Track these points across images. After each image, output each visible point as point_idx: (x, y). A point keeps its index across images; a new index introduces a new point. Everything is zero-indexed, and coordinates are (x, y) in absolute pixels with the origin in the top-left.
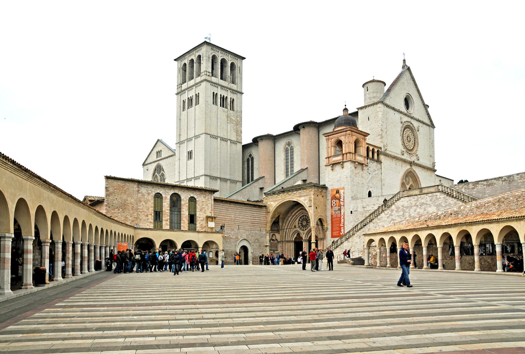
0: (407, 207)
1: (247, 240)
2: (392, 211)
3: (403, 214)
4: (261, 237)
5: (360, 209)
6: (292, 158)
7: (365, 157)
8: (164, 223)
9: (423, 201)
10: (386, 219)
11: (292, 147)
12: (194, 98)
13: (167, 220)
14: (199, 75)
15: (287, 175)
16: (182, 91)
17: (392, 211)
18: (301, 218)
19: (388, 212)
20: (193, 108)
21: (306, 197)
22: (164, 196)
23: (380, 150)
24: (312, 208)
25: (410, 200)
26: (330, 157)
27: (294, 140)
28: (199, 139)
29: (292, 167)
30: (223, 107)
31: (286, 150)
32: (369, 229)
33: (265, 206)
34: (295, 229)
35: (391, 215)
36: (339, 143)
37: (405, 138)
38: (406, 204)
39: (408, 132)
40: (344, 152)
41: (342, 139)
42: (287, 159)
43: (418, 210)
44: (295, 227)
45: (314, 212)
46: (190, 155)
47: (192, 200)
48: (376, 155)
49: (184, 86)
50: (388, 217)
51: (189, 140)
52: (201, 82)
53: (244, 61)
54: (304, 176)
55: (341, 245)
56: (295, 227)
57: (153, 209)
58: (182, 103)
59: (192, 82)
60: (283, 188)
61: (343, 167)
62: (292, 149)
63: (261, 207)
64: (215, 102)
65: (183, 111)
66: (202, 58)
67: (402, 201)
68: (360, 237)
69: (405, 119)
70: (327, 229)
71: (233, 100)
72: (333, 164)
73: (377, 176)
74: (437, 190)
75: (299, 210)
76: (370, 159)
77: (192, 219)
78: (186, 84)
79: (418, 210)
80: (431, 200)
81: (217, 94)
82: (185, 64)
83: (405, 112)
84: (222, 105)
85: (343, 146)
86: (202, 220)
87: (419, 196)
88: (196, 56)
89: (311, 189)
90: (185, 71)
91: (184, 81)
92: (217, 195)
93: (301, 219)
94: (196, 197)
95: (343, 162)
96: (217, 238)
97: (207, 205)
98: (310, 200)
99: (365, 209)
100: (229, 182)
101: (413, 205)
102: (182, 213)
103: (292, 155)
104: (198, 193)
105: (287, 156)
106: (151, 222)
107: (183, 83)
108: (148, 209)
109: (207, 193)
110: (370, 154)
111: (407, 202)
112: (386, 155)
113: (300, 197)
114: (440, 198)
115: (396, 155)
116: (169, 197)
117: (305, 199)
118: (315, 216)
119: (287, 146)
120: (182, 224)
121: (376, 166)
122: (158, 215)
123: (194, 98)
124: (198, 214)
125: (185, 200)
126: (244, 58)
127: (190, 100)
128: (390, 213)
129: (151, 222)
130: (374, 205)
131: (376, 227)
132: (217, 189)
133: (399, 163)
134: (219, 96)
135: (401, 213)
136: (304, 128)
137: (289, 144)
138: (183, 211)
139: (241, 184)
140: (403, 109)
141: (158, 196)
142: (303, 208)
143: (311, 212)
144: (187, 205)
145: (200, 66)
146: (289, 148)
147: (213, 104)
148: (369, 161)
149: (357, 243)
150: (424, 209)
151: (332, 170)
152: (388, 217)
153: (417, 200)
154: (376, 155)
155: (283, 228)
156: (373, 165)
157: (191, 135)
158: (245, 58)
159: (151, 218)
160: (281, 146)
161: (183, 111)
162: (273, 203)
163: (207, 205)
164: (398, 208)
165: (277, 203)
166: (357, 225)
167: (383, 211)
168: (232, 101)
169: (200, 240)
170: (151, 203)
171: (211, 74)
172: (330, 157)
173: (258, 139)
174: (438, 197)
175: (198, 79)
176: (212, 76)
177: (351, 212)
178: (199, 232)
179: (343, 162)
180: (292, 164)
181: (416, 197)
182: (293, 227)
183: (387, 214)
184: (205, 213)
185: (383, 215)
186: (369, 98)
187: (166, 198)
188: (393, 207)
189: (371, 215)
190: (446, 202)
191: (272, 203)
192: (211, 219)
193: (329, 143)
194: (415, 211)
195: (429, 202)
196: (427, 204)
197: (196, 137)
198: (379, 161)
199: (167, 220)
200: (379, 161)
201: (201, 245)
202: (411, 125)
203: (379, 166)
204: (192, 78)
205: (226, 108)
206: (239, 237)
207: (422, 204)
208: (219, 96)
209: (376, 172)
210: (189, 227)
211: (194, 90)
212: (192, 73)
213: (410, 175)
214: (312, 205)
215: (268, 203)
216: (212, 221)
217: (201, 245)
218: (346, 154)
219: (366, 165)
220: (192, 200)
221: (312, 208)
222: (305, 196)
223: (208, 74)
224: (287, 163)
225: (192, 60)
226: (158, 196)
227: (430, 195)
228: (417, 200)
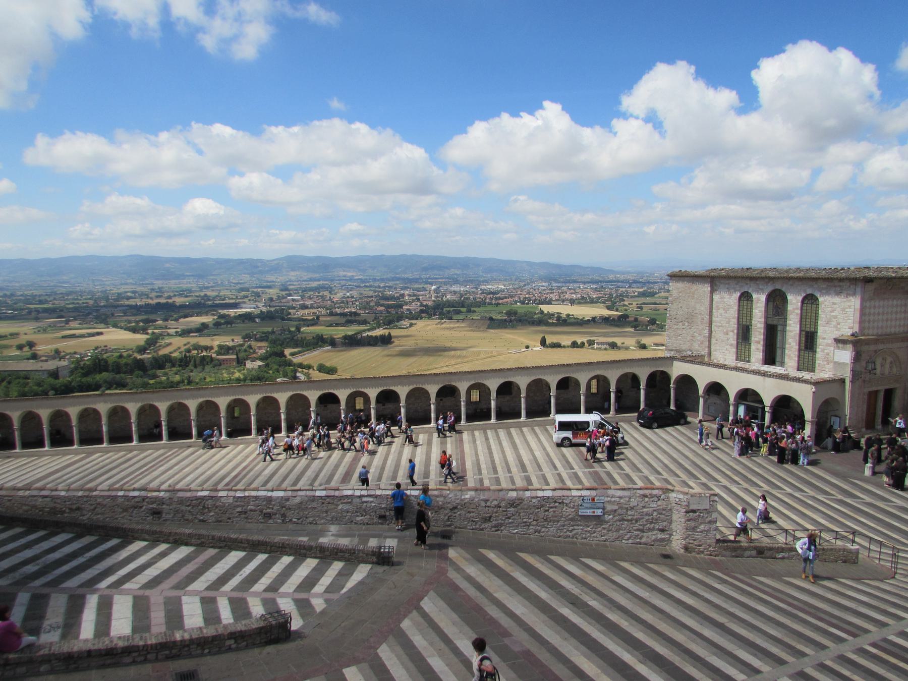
8: (753, 347)
13: (758, 342)
22: (755, 296)
47: (810, 300)
57: (735, 321)
77: (809, 341)
86: (828, 345)
94: (817, 295)
97: (843, 310)
102: (788, 328)
106: (731, 345)
108: (728, 322)
116: (763, 298)
120: (787, 351)
122: (744, 333)
129: (731, 345)
141: (746, 297)
144: (799, 312)
159: (732, 338)
163: (843, 310)
170: (733, 312)
184: (838, 330)
187: (758, 299)
192: (840, 345)
199: (758, 342)
201: (768, 401)
216: (843, 349)
217: (768, 401)
220: (810, 300)
226: (746, 297)
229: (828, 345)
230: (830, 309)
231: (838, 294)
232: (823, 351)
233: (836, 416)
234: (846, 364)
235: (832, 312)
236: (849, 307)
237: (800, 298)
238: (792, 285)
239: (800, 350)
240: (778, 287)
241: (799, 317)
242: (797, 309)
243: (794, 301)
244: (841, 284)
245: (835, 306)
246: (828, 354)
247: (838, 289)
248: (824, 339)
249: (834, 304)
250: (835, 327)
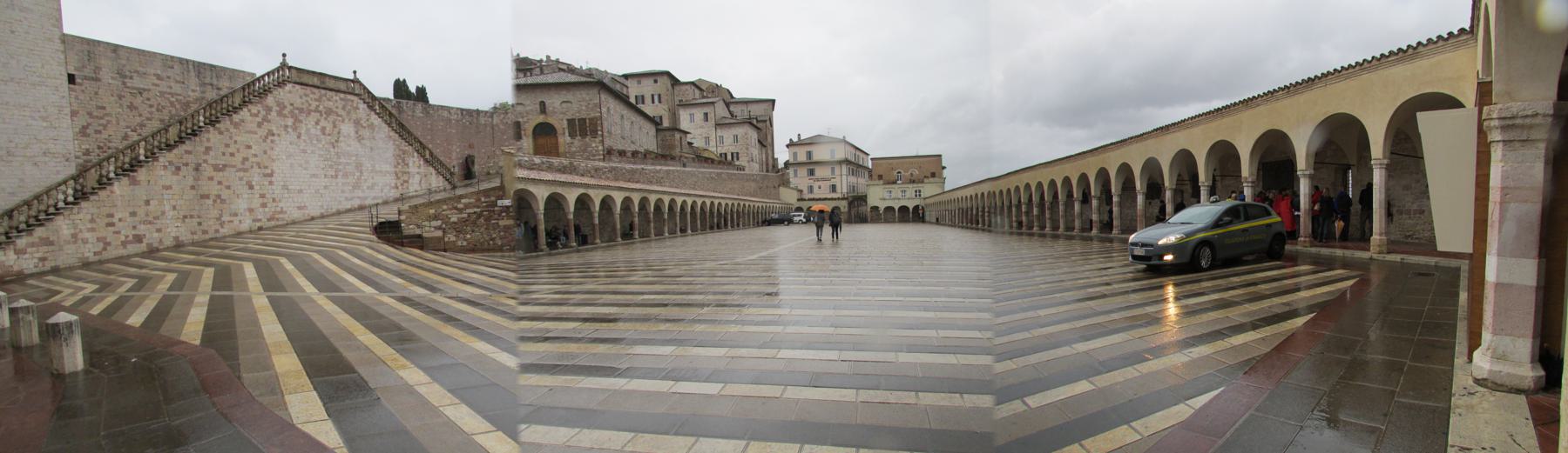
0: (301, 110)
2: (269, 109)
10: (253, 126)
17: (269, 109)
32: (208, 149)
35: (265, 119)
38: (298, 102)
43: (323, 123)
50: (260, 125)
68: (178, 169)
79: (323, 123)
131: (227, 146)
149: (169, 188)
153: (319, 100)
164: (282, 106)
195: (340, 112)
207: (329, 112)
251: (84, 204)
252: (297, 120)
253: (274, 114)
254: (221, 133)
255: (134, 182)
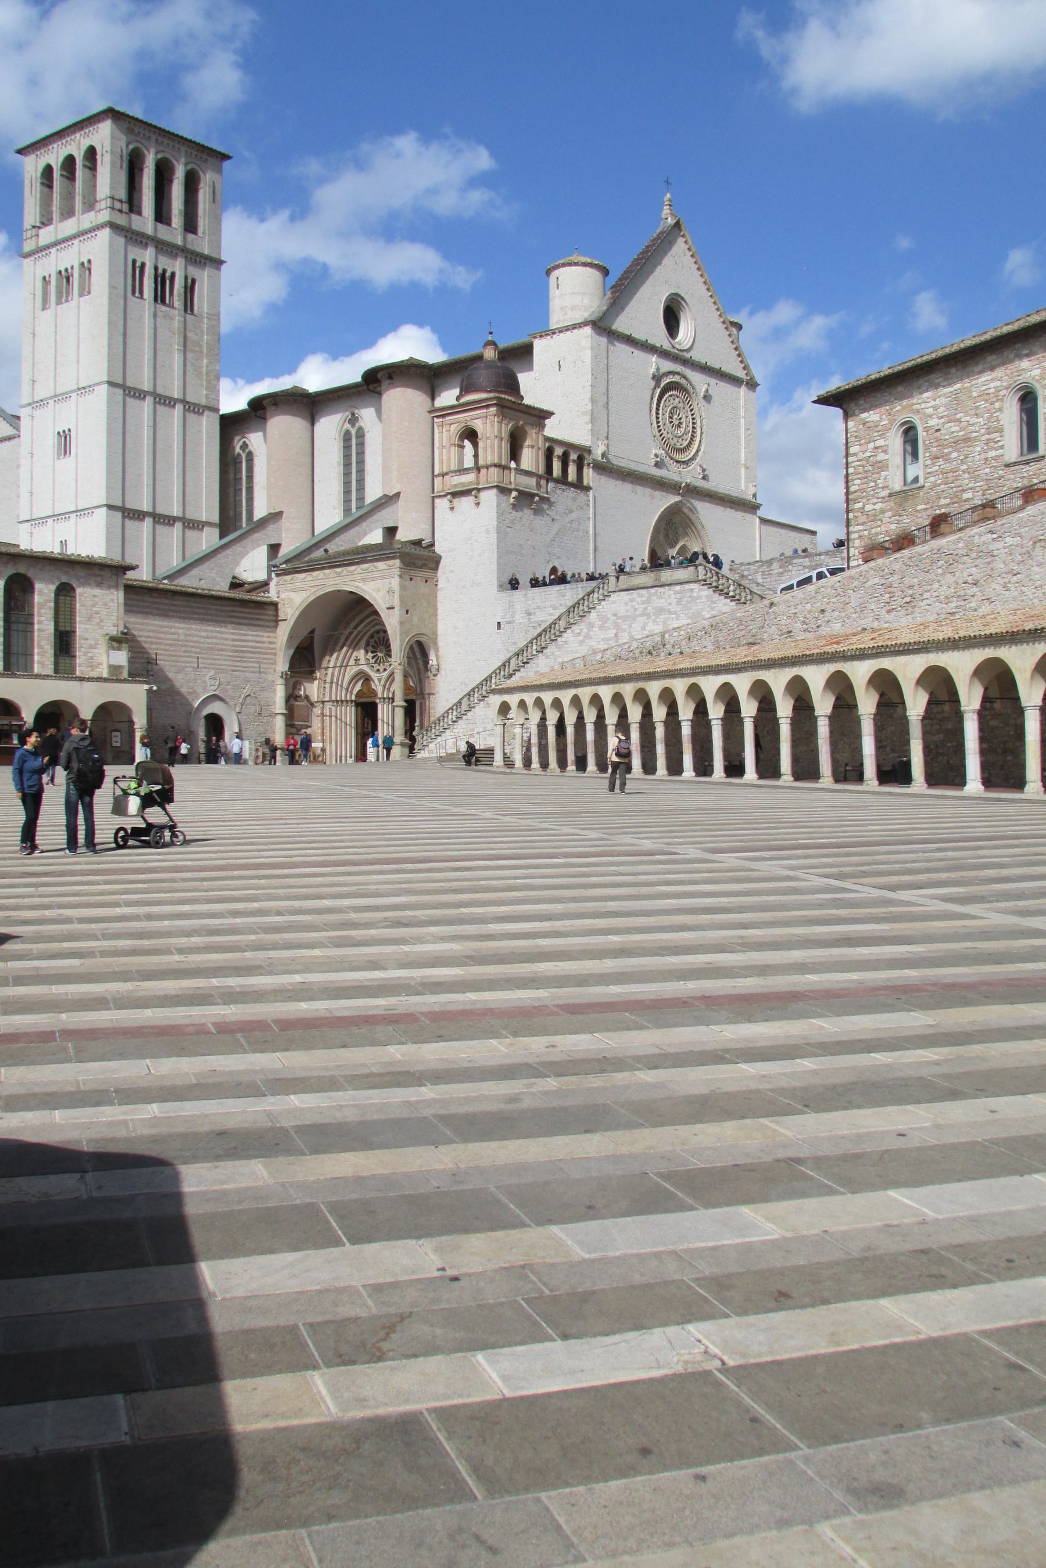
0: (625, 618)
1: (221, 699)
2: (591, 625)
3: (616, 635)
4: (263, 689)
5: (520, 618)
6: (361, 462)
7: (539, 477)
9: (662, 603)
11: (360, 429)
12: (76, 274)
14: (90, 205)
15: (347, 511)
16: (39, 250)
18: (372, 637)
19: (579, 628)
20: (73, 304)
21: (379, 583)
23: (586, 455)
24: (396, 611)
25: (631, 600)
26: (446, 474)
27: (367, 415)
28: (90, 397)
29: (361, 487)
30: (163, 301)
31: (347, 438)
33: (275, 605)
34: (355, 669)
35: (587, 637)
36: (470, 435)
37: (665, 418)
38: (622, 610)
39: (674, 399)
40: (481, 462)
41: (478, 425)
42: (347, 465)
44: (357, 660)
45: (401, 623)
46: (65, 440)
47: (65, 591)
48: (572, 469)
49: (47, 235)
50: (581, 643)
51: (60, 397)
52: (98, 228)
53: (227, 164)
54: (386, 517)
55: (469, 714)
56: (357, 660)
58: (39, 284)
59: (69, 227)
60: (326, 551)
61: (478, 504)
62: (361, 434)
63: (261, 605)
64: (137, 289)
65: (44, 309)
66: (99, 157)
67: (614, 602)
69: (667, 366)
70: (438, 670)
71: (194, 281)
72: (455, 495)
73: (574, 525)
74: (692, 578)
75: (368, 616)
76: (557, 481)
77: (64, 643)
78: (51, 228)
80: (679, 603)
81: (143, 265)
82: (48, 170)
83: (667, 346)
84: (160, 297)
85: (481, 444)
86: (91, 647)
87: (653, 590)
88: (84, 149)
89: (391, 562)
90: (50, 186)
91: (46, 221)
92: (130, 575)
93: (372, 642)
95: (479, 490)
96: (135, 697)
97: (106, 604)
98: (390, 591)
99: (534, 619)
100: (178, 526)
101: (638, 612)
103: (361, 453)
104: (81, 572)
105: (347, 456)
107: (44, 224)
109: (107, 573)
110: (557, 466)
111: (626, 604)
112: (604, 468)
113: (364, 580)
114: (699, 597)
115: (633, 466)
117: (380, 586)
118: (403, 633)
119: (347, 426)
121: (574, 500)
123: (76, 274)
124: (80, 629)
125: (46, 591)
126: (225, 157)
127: (66, 277)
128: (585, 630)
130: (554, 607)
132: (134, 563)
133: (643, 493)
134: (149, 272)
135: (611, 633)
136: (390, 377)
137: (353, 420)
138: (40, 622)
139: (216, 532)
140: (659, 336)
142: (376, 613)
143: (392, 622)
144: (52, 605)
145: (95, 176)
146: (353, 432)
147: (134, 292)
148: (551, 485)
150: (664, 623)
151: (452, 509)
152: (581, 643)
154: (572, 469)
155: (324, 665)
156: (562, 497)
157: (68, 383)
158: (225, 157)
160: (330, 426)
161: (44, 309)
162: (294, 596)
163: (106, 604)
164: (604, 619)
165: (304, 595)
166: (509, 661)
167: (569, 625)
168: (190, 289)
169: (86, 700)
171: (125, 207)
172: (446, 474)
173: (265, 402)
174: (695, 594)
175: (87, 220)
176: (131, 210)
177: (499, 623)
178: (81, 679)
179: (479, 490)
180: (361, 481)
181: (644, 592)
182: (352, 662)
183: (579, 634)
184: (101, 628)
185: (568, 635)
186: (562, 309)
188: (593, 615)
189: (540, 635)
190: (712, 609)
191: (292, 595)
192: (115, 644)
193: (445, 433)
194: (643, 628)
195: (673, 608)
196: (670, 612)
197: (82, 390)
198: (579, 485)
200: (579, 485)
201: (86, 713)
202: (683, 381)
203: (581, 496)
204: (68, 212)
205: (171, 306)
206: (199, 690)
207: (660, 611)
208: (149, 272)
209: (574, 516)
210: (56, 664)
211: (75, 248)
212: (69, 197)
213: (673, 526)
214: (397, 603)
215: (283, 596)
216: (119, 649)
217: (86, 713)
218: (487, 467)
219: (542, 499)
220: (65, 591)
221: (396, 611)
222: (377, 578)
223: (118, 205)
224: (347, 474)
225: (69, 162)
227: (678, 588)
228: (648, 601)
229: (91, 647)
230: (90, 603)
231: (99, 585)
232: (85, 654)
233: (116, 730)
234: (120, 667)
235: (93, 606)
236: (112, 600)
237: (53, 587)
238: (41, 569)
239: (56, 655)
240: (22, 569)
241: (52, 612)
242: (50, 601)
243: (43, 593)
244: (102, 573)
245: (96, 599)
246: (92, 658)
247: (99, 579)
248: (86, 639)
249: (95, 596)
250: (98, 624)
251: (460, 722)
252: (618, 627)
253: (596, 629)
254: (547, 657)
255: (488, 705)
